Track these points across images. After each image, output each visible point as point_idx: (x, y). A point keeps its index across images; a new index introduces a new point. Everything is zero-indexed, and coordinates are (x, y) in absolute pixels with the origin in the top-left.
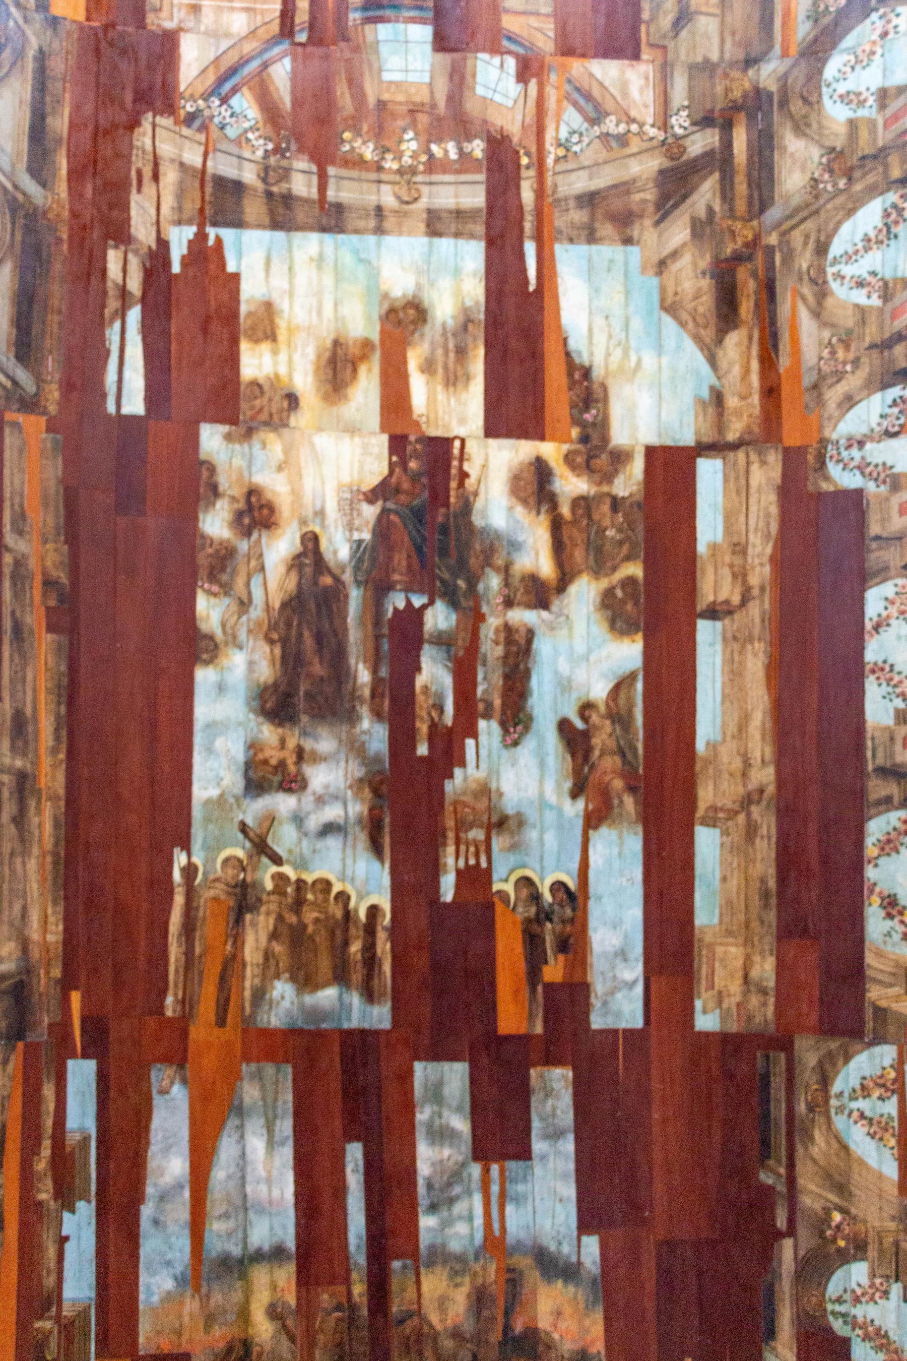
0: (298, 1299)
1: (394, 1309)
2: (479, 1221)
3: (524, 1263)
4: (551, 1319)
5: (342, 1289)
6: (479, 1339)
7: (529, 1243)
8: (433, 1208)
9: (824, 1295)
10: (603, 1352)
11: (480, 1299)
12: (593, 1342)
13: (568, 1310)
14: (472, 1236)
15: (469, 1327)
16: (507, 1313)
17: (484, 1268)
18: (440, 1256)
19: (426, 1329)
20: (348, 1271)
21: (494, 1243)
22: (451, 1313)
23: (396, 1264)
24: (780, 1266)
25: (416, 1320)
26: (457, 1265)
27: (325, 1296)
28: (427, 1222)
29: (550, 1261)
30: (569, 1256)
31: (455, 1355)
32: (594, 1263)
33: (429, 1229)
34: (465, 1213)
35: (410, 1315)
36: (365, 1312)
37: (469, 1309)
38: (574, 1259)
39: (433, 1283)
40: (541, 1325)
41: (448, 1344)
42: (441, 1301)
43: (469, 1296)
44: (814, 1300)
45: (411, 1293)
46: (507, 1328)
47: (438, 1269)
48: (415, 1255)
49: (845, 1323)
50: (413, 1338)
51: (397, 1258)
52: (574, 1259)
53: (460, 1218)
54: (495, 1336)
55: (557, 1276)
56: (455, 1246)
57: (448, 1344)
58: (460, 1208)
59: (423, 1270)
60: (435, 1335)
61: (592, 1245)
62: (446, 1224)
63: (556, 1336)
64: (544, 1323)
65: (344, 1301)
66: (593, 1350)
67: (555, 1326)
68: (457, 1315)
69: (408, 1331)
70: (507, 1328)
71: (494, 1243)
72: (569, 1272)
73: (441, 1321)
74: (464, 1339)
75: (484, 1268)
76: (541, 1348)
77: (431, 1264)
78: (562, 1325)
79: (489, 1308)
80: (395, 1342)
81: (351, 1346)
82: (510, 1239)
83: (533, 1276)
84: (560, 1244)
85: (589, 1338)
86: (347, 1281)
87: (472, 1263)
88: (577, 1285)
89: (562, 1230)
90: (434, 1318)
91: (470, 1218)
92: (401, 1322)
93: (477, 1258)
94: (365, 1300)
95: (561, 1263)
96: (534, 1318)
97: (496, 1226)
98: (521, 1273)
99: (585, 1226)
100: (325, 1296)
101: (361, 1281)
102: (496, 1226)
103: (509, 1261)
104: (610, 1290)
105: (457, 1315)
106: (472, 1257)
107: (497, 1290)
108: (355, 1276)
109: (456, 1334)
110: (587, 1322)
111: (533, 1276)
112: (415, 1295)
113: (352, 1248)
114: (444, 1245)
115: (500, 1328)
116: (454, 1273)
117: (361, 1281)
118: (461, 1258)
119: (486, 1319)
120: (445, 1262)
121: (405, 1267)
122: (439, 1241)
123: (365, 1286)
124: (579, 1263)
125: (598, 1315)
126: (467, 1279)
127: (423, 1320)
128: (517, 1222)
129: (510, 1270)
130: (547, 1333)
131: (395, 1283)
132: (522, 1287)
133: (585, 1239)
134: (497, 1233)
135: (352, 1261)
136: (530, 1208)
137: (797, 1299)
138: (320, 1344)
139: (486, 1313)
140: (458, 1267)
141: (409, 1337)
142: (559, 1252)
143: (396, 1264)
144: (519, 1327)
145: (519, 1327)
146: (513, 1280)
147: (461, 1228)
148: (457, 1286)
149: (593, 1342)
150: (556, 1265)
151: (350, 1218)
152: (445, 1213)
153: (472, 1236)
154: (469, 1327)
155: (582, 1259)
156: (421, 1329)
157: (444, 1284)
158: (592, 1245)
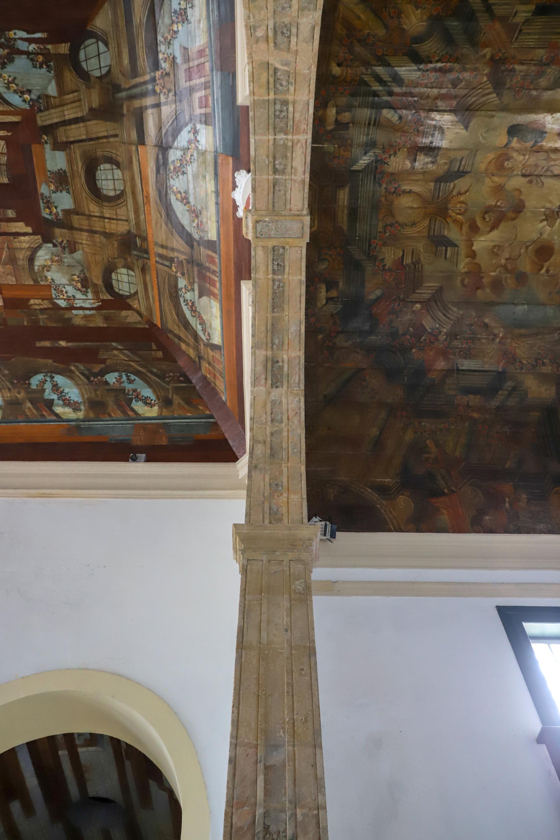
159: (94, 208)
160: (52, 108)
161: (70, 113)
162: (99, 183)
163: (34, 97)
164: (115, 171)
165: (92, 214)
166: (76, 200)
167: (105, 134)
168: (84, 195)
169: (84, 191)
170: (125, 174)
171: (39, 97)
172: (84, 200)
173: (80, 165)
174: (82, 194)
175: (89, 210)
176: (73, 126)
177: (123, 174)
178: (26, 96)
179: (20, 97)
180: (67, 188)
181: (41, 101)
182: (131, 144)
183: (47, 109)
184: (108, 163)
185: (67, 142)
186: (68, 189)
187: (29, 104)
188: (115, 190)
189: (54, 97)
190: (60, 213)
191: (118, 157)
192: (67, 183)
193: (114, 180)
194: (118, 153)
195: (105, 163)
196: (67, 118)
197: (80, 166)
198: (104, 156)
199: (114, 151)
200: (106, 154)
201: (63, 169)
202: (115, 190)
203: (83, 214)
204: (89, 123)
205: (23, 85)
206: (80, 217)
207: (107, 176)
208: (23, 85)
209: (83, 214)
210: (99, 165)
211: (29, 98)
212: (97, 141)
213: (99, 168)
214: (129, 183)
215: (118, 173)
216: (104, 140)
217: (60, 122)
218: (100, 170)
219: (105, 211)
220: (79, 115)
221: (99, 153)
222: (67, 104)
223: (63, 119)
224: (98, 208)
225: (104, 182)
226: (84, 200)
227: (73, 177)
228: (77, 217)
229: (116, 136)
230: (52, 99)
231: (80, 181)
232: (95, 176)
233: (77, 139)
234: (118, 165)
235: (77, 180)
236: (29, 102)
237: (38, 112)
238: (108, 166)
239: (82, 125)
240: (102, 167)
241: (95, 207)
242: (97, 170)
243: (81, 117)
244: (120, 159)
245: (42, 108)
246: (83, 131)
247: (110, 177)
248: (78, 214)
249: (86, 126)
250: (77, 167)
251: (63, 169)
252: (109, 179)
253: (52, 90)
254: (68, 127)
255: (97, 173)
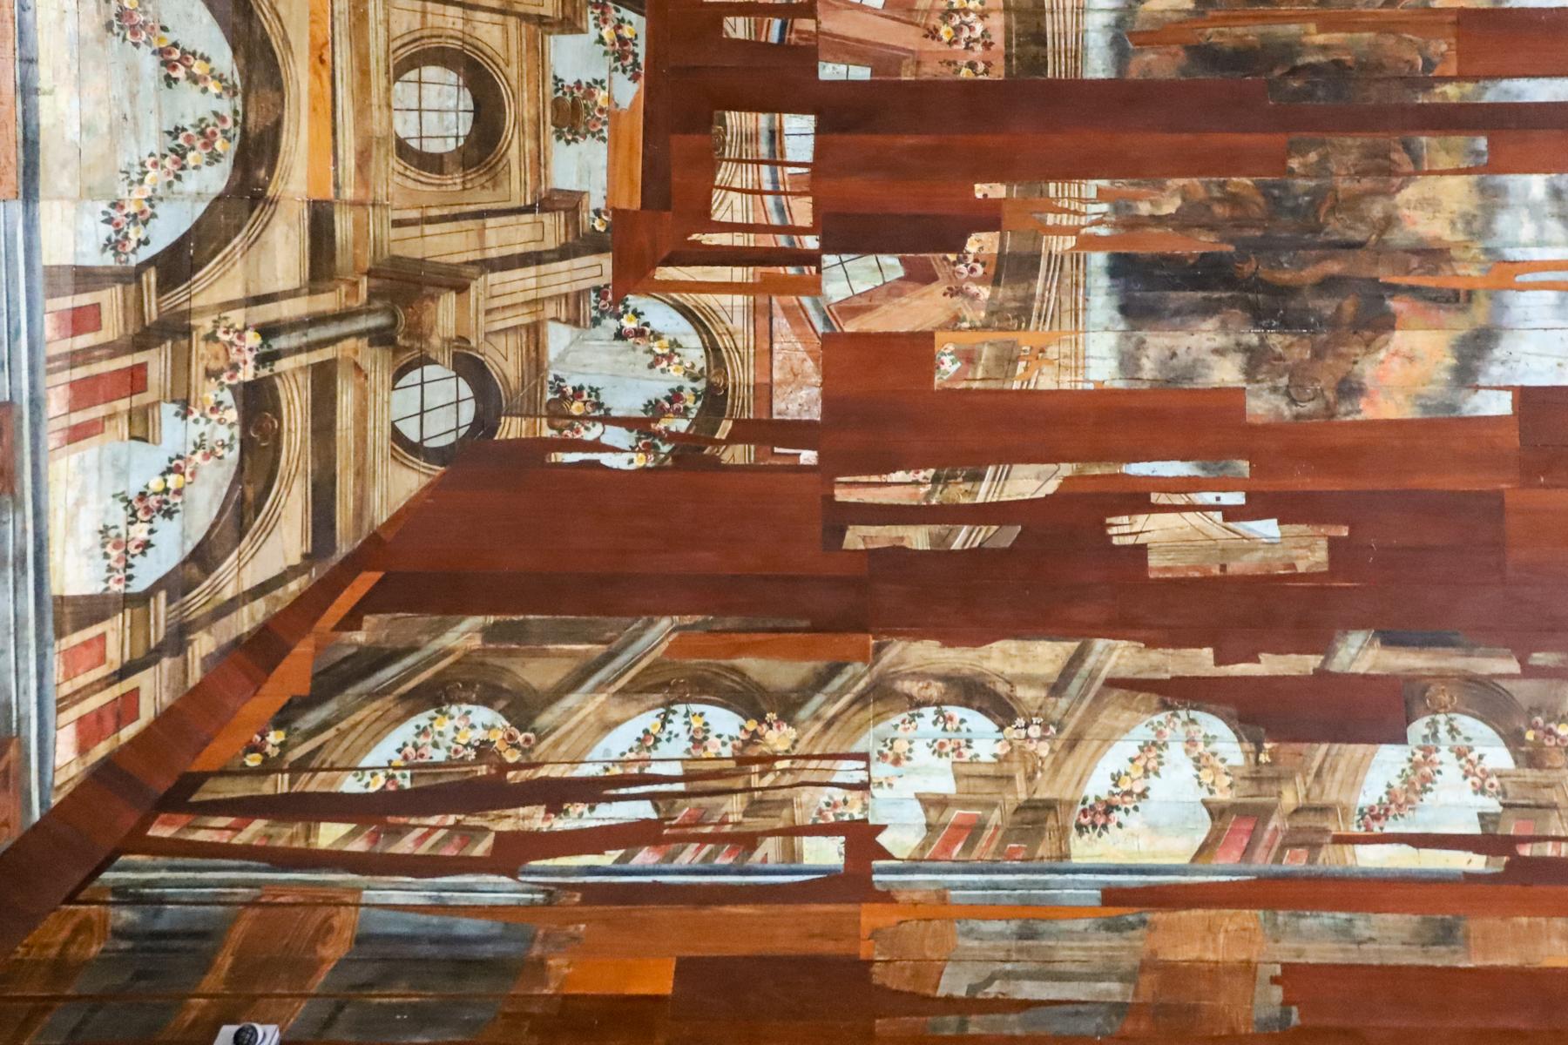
0: (1441, 10)
1: (1424, 139)
2: (1536, 254)
3: (1480, 314)
4: (1405, 349)
5: (1452, 70)
6: (1382, 250)
7: (1505, 322)
8: (1556, 193)
9: (1455, 711)
10: (1359, 417)
11: (1433, 254)
12: (1372, 403)
13: (1416, 371)
14: (1516, 245)
15: (1397, 237)
16: (1412, 290)
17: (1474, 260)
18: (1492, 200)
19: (1397, 181)
20: (1475, 79)
21: (1507, 274)
22: (1417, 215)
23: (1482, 143)
24: (1483, 655)
25: (1411, 168)
26: (1480, 224)
27: (1444, 47)
28: (1536, 185)
29: (1480, 349)
30: (1486, 374)
31: (1362, 220)
32: (1477, 408)
33: (1527, 189)
34: (1547, 236)
35: (1416, 161)
36: (1422, 99)
37: (1421, 240)
38: (1482, 381)
39: (1456, 192)
40: (1397, 334)
41: (1377, 210)
42: (1433, 203)
43: (1439, 239)
44: (1446, 698)
45: (1444, 162)
46: (1395, 289)
47: (1476, 199)
48: (1494, 168)
49: (1425, 737)
50: (1387, 163)
51: (1491, 144)
52: (1482, 381)
53: (1541, 229)
54: (1385, 275)
55: (1461, 357)
56: (1504, 222)
57: (1377, 210)
58: (1554, 228)
59: (1473, 178)
60: (1389, 193)
61: (1499, 405)
62: (1534, 210)
63: (1382, 355)
64: (1400, 339)
65: (1436, 73)
66: (1363, 403)
67: (1395, 354)
68: (1415, 223)
69: (1395, 156)
70: (1395, 289)
71: (1507, 274)
72: (1465, 374)
73: (1408, 201)
74: (1382, 232)
75: (1474, 260)
76: (1368, 334)
77: (1482, 189)
78: (1396, 364)
79: (1420, 267)
80: (1381, 138)
81: (1377, 80)
82: (1510, 296)
83: (1461, 324)
84: (1503, 363)
85: (1380, 398)
86: (1460, 78)
87: (1481, 245)
88: (1448, 383)
89: (1521, 367)
90: (1410, 193)
91: (1540, 243)
92: (1407, 148)
93: (1487, 251)
94: (1438, 100)
95: (1476, 363)
96: (1406, 327)
97: (1528, 278)
98: (1463, 310)
99: (1527, 398)
100: (1444, 47)
101: (1463, 96)
102: (1528, 278)
103: (1481, 293)
104: (1439, 431)
105: (1415, 223)
106: (1489, 244)
107: (1441, 280)
108: (1469, 87)
109: (1389, 221)
110: (1400, 397)
111: (1461, 324)
112: (1441, 167)
113: (1505, 84)
114: (1504, 207)
115: (1395, 280)
116: (1468, 220)
117: (1463, 96)
118: (1487, 231)
119: (1408, 263)
120: (1483, 207)
121: (1478, 154)
122: (1511, 201)
123: (1454, 101)
124: (1478, 388)
125: (1409, 412)
126: (1460, 237)
127: (1409, 177)
128: (1532, 307)
129: (1470, 295)
130: (1387, 343)
131: (1458, 140)
132: (1448, 310)
133: (1508, 396)
134: (1518, 279)
135: (1488, 83)
136: (1551, 323)
137: (1441, 676)
138: (1382, 40)
139: (1415, 262)
140: (1477, 225)
141: (1387, 157)
142: (1491, 362)
143: (1482, 143)
144: (1395, 304)
145: (1395, 304)
146: (1457, 299)
147: (1527, 231)
148: (1453, 223)
149: (1372, 403)
150: (1475, 357)
151: (1546, 81)
152: (1547, 209)
153: (1516, 245)
154: (1397, 237)
155: (1482, 392)
156: (1397, 175)
157: (1455, 207)
158: (1499, 405)
159: (490, 33)
160: (566, 296)
161: (522, 281)
162: (467, 101)
163: (611, 324)
164: (414, 134)
165: (497, 18)
166: (538, 54)
167: (429, 229)
168: (513, 72)
169: (514, 83)
170: (384, 124)
171: (596, 322)
172: (514, 59)
173: (514, 152)
174: (520, 76)
175: (504, 25)
176: (519, 249)
177: (391, 124)
178: (629, 324)
179: (647, 324)
180: (560, 94)
181: (594, 313)
182: (358, 204)
183: (579, 295)
184: (432, 155)
185: (543, 210)
186: (557, 91)
187: (627, 307)
188: (420, 82)
189: (556, 319)
190: (592, 23)
191: (401, 169)
192: (556, 103)
193: (420, 110)
194: (398, 179)
195: (441, 156)
196: (532, 271)
197: (515, 147)
198: (441, 172)
199: (410, 184)
200: (435, 178)
201: (562, 142)
202: (420, 82)
203: (524, 17)
204: (477, 256)
205: (634, 349)
206: (533, 10)
207: (441, 120)
208: (634, 349)
209: (524, 17)
210: (458, 149)
211: (624, 321)
212: (456, 210)
213: (461, 142)
214: (375, 101)
215: (406, 127)
216: (434, 212)
217: (552, 261)
218: (457, 137)
219: (459, 25)
220: (495, 277)
221: (454, 180)
222: (526, 303)
223: (543, 268)
224: (477, 34)
225: (451, 103)
226: (514, 59)
227: (537, 122)
228: (543, 12)
229: (398, 224)
230: (563, 318)
231: (520, 107)
232: (475, 121)
233: (513, 219)
234: (403, 149)
235: (528, 112)
236: (626, 312)
237: (606, 286)
238: (433, 147)
239: (492, 254)
240: (451, 145)
241: (486, 38)
242: (467, 138)
243: (493, 271)
244: (395, 163)
245: (593, 295)
246: (492, 238)
247: (431, 119)
248: (541, 20)
249: (483, 249)
250: (521, 147)
251: (562, 142)
252: (437, 110)
253: (558, 338)
254: (532, 247)
255: (468, 130)
